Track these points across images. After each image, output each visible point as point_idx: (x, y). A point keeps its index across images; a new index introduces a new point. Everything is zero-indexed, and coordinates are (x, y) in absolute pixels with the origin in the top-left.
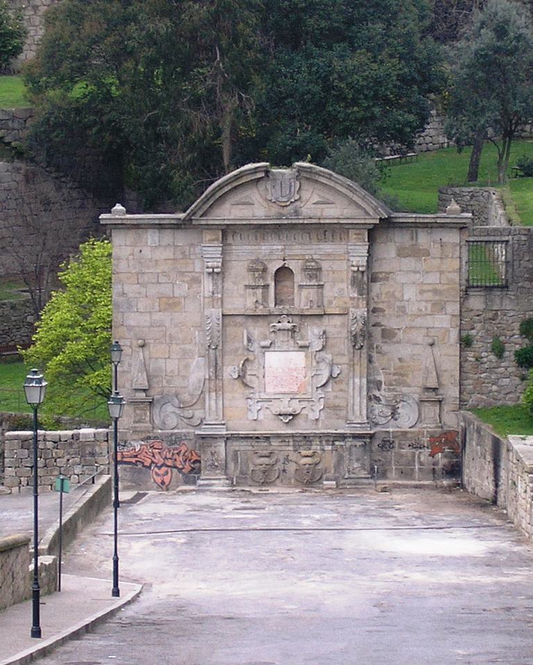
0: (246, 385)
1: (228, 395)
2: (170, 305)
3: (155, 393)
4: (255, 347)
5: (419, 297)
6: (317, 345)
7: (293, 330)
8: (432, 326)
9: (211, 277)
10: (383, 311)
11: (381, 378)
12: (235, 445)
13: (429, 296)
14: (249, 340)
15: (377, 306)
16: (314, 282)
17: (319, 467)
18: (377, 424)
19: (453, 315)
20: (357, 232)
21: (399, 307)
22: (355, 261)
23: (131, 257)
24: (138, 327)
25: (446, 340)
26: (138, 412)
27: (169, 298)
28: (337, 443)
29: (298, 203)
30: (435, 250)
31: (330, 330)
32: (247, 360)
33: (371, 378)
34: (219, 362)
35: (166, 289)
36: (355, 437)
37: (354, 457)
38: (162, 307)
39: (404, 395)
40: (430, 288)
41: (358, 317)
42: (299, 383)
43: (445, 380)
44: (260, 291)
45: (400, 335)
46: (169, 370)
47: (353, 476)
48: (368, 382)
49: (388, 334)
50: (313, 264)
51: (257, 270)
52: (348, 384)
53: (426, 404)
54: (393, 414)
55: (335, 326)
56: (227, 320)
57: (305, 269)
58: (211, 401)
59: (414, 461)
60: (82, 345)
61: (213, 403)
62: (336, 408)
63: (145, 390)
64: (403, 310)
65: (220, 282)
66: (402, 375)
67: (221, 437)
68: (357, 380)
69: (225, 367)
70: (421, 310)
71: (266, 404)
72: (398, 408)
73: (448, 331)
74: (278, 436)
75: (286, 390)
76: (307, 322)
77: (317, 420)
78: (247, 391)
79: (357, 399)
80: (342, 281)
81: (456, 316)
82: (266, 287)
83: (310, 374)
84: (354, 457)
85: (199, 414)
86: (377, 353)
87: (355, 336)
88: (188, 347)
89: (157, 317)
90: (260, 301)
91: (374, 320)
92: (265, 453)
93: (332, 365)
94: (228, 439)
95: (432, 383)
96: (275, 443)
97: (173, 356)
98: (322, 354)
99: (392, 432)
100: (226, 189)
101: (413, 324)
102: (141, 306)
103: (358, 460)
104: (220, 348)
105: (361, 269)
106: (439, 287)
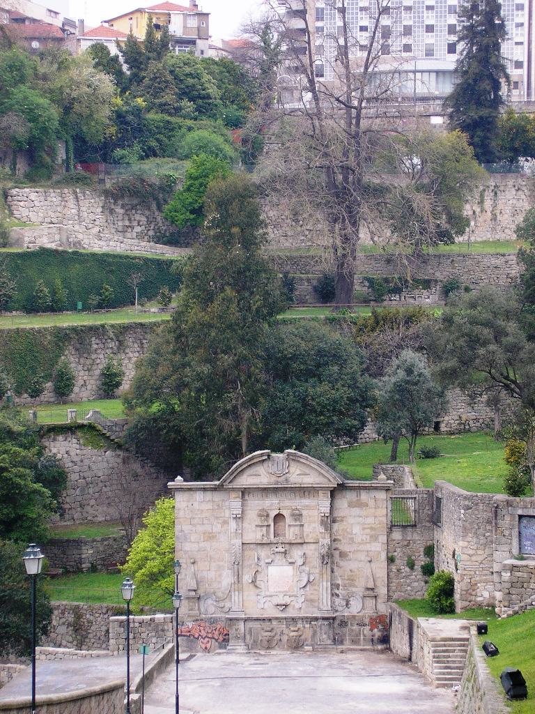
0: (256, 587)
1: (246, 593)
2: (210, 537)
3: (201, 592)
4: (262, 563)
6: (300, 562)
7: (285, 553)
9: (235, 520)
10: (340, 541)
11: (339, 582)
12: (250, 624)
13: (368, 531)
14: (258, 559)
16: (298, 523)
17: (302, 637)
18: (337, 611)
20: (324, 492)
21: (349, 538)
22: (323, 510)
23: (186, 509)
24: (191, 551)
25: (379, 559)
26: (191, 604)
27: (210, 533)
28: (313, 623)
29: (287, 475)
30: (371, 503)
31: (309, 553)
32: (257, 571)
33: (334, 582)
34: (240, 573)
35: (208, 528)
36: (324, 619)
37: (323, 632)
38: (206, 539)
39: (354, 593)
40: (369, 526)
43: (378, 583)
44: (264, 529)
45: (351, 555)
46: (209, 577)
47: (322, 643)
48: (332, 585)
49: (343, 555)
50: (297, 512)
51: (263, 516)
52: (319, 586)
53: (368, 598)
54: (347, 605)
55: (311, 550)
56: (245, 546)
57: (293, 515)
58: (236, 597)
60: (157, 562)
61: (236, 598)
62: (312, 601)
63: (195, 591)
64: (352, 539)
65: (240, 523)
66: (352, 580)
67: (242, 619)
68: (325, 583)
69: (244, 576)
70: (363, 540)
71: (269, 599)
73: (379, 552)
74: (277, 618)
75: (282, 590)
76: (294, 548)
77: (300, 608)
78: (258, 591)
80: (315, 522)
82: (268, 526)
83: (296, 580)
84: (323, 632)
85: (228, 605)
87: (323, 556)
88: (221, 563)
89: (202, 545)
90: (265, 535)
91: (334, 546)
92: (269, 629)
93: (309, 574)
94: (246, 620)
95: (371, 585)
96: (274, 623)
98: (303, 567)
100: (244, 466)
101: (359, 549)
103: (325, 633)
104: (241, 563)
105: (326, 515)
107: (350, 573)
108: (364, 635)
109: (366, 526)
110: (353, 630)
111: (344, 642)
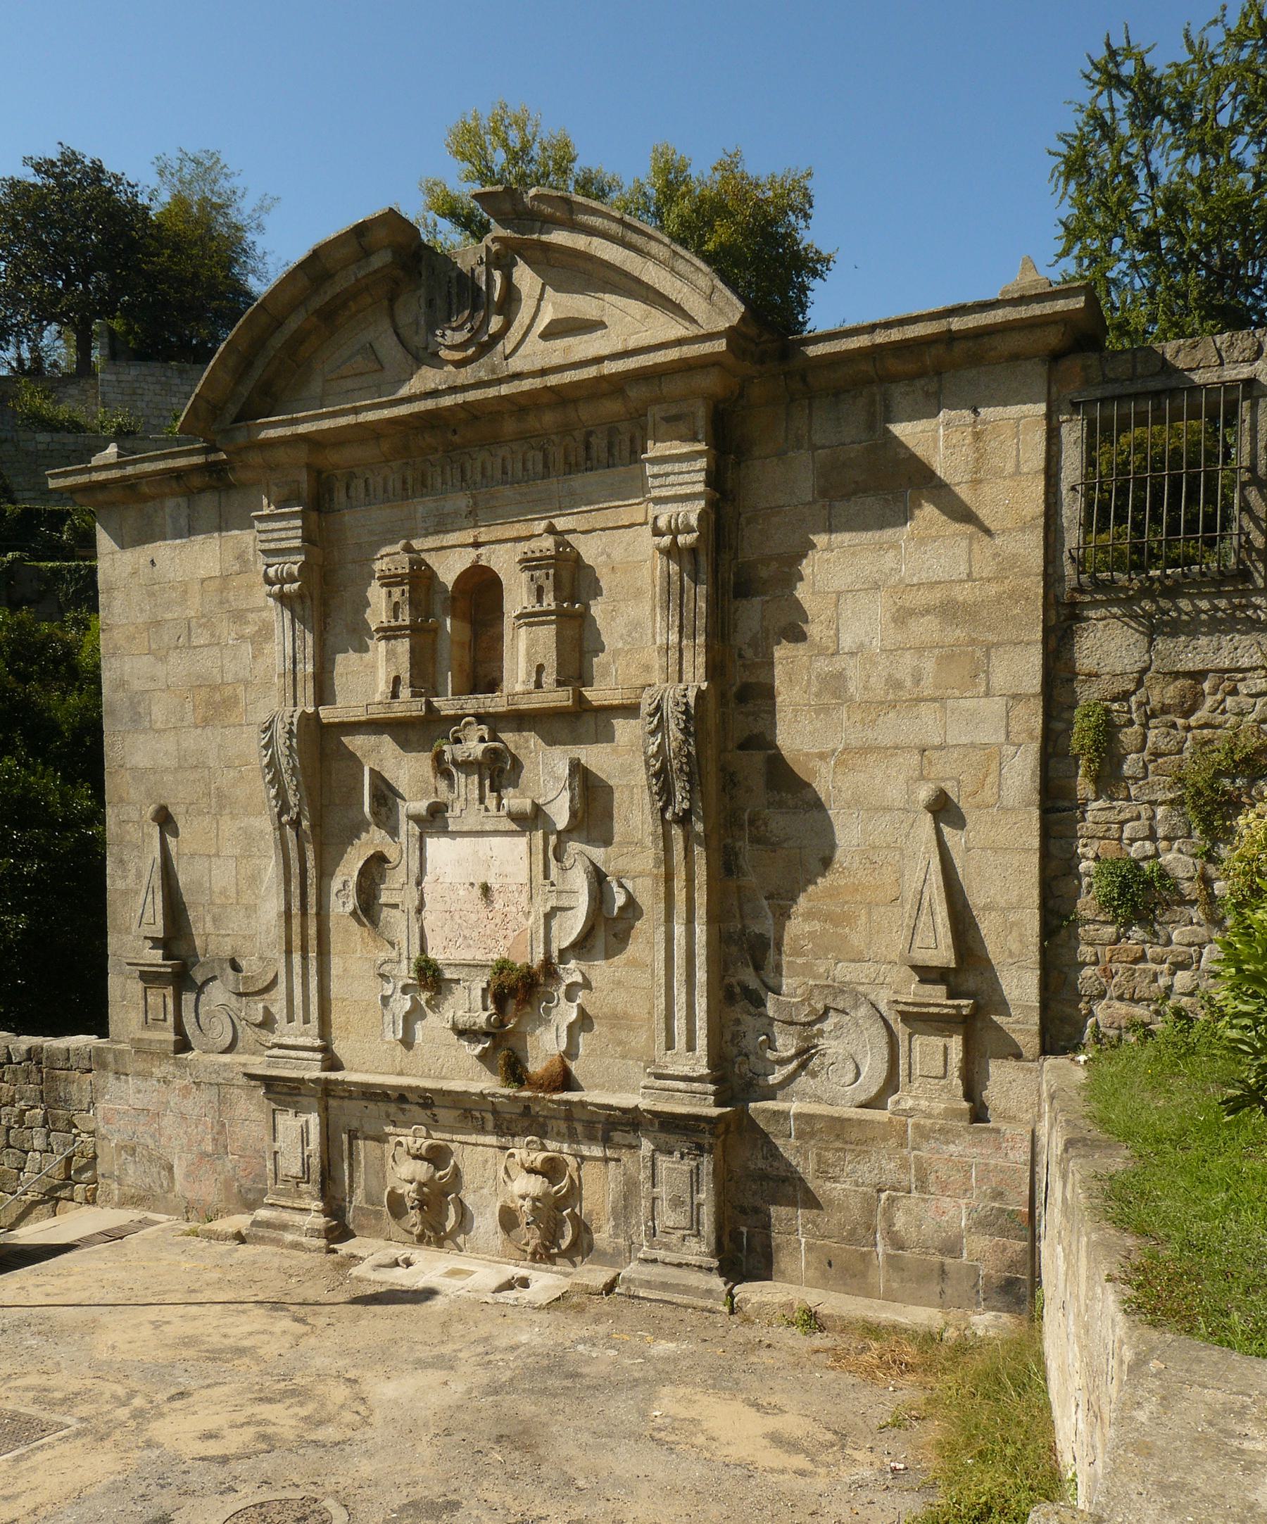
8: (937, 741)
15: (753, 680)
19: (1015, 697)
27: (215, 688)
35: (207, 662)
41: (668, 707)
42: (511, 935)
59: (870, 1228)
72: (821, 1033)
81: (1028, 697)
84: (662, 1191)
86: (755, 840)
99: (799, 1116)
102: (159, 713)
106: (964, 593)
108: (897, 1242)
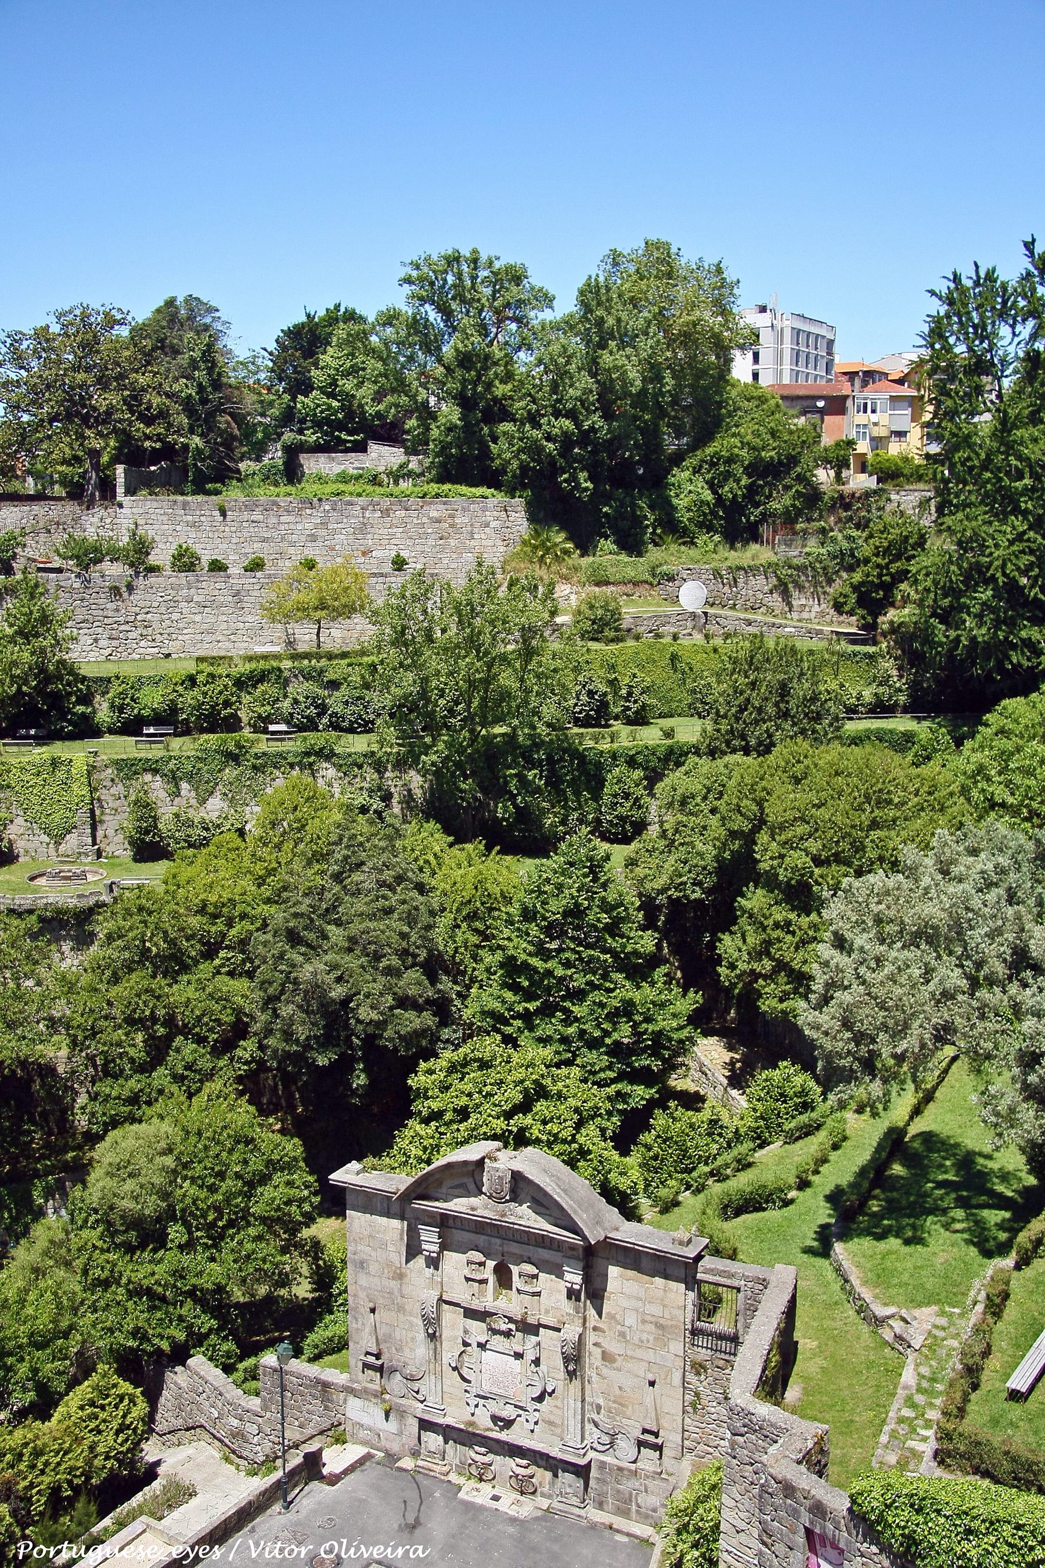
5: (641, 1327)
43: (665, 1423)
64: (622, 1335)
68: (572, 1402)
79: (572, 1422)
97: (401, 1325)
107: (618, 1392)
109: (648, 1318)
110: (618, 1491)
111: (605, 1507)
